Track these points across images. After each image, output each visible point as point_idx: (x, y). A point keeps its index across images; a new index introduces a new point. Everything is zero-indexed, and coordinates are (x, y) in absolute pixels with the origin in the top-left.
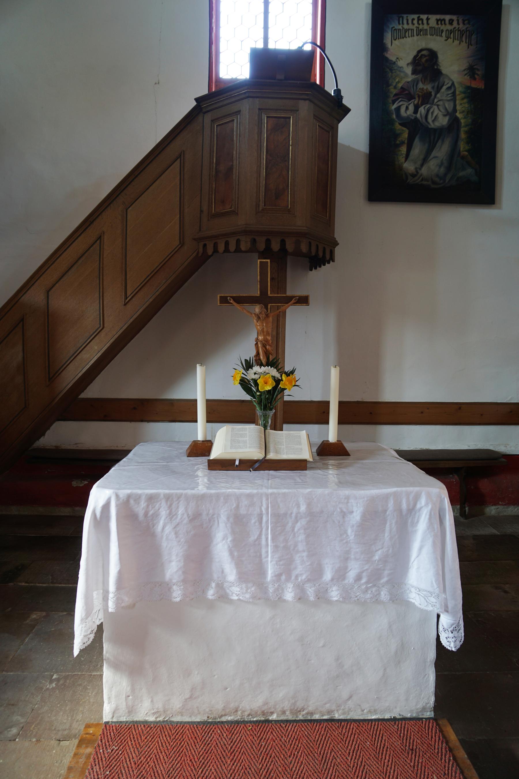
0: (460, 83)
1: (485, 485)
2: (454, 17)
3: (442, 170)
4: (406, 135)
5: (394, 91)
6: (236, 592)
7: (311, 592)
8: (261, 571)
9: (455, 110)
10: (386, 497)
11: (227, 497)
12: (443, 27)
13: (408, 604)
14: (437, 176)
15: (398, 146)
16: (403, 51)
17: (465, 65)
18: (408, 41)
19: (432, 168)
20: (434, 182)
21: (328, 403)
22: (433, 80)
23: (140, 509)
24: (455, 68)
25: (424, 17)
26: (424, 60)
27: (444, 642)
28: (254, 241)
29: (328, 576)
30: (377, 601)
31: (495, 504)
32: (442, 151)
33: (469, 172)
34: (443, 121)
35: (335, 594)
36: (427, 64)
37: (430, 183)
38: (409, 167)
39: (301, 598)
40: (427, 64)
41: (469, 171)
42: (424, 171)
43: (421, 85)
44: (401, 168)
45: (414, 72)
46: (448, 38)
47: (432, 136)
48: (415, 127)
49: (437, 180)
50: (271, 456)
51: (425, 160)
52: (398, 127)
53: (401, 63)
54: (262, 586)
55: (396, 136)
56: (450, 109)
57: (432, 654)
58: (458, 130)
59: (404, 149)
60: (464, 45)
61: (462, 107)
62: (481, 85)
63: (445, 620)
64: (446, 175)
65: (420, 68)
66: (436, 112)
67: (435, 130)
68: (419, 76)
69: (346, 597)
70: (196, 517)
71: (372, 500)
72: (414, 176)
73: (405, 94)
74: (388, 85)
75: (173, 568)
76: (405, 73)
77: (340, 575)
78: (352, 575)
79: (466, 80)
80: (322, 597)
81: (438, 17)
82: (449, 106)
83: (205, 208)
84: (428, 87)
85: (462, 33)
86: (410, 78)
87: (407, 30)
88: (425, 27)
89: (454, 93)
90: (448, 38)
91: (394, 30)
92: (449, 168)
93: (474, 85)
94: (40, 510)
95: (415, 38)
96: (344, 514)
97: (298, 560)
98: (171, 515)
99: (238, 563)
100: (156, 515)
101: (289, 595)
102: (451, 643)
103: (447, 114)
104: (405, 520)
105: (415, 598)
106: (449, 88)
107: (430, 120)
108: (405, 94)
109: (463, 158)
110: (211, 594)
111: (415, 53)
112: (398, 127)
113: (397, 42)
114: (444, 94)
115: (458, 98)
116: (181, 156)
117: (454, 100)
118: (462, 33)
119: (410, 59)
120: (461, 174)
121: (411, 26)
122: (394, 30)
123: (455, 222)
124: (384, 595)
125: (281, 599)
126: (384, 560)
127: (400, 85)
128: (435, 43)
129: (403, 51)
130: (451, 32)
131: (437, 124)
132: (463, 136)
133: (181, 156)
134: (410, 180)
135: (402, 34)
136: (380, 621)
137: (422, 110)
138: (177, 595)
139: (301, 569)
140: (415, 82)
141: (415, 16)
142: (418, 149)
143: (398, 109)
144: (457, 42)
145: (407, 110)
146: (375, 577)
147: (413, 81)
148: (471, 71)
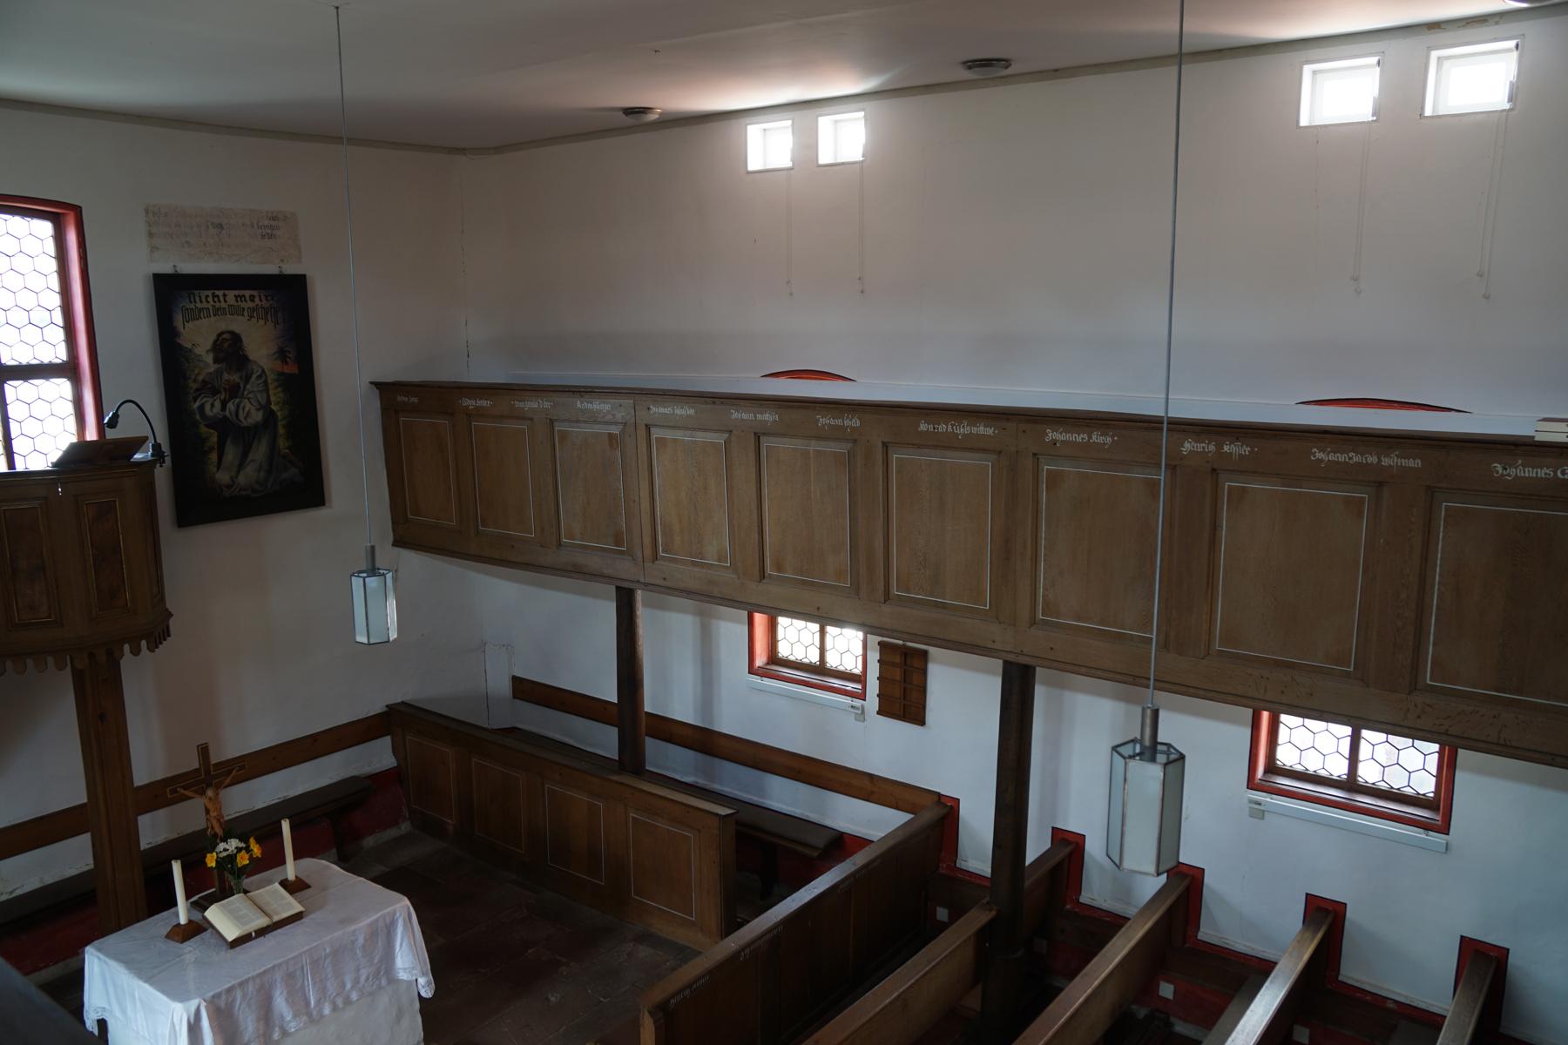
2: (255, 293)
3: (262, 474)
4: (215, 439)
5: (194, 386)
7: (340, 1002)
8: (308, 1004)
9: (269, 402)
10: (377, 921)
12: (243, 305)
13: (399, 981)
16: (199, 336)
18: (204, 321)
21: (296, 858)
23: (222, 1003)
25: (220, 293)
27: (423, 994)
29: (349, 986)
30: (380, 987)
32: (260, 452)
34: (257, 417)
35: (354, 996)
36: (230, 350)
38: (223, 477)
39: (335, 1008)
40: (230, 350)
42: (242, 479)
43: (226, 376)
45: (216, 361)
46: (251, 317)
48: (225, 427)
50: (276, 918)
51: (241, 466)
52: (203, 429)
53: (198, 351)
54: (309, 1015)
56: (263, 400)
57: (417, 1005)
59: (214, 456)
61: (276, 396)
63: (422, 981)
66: (248, 406)
67: (248, 428)
71: (370, 925)
72: (229, 487)
73: (209, 388)
77: (356, 981)
78: (363, 978)
80: (348, 1002)
81: (237, 292)
82: (262, 398)
84: (235, 378)
87: (201, 310)
88: (223, 305)
89: (266, 382)
90: (251, 317)
93: (287, 370)
95: (213, 319)
96: (353, 942)
97: (329, 984)
98: (244, 996)
100: (234, 1000)
102: (427, 993)
103: (261, 407)
104: (390, 929)
105: (403, 976)
106: (259, 377)
107: (241, 417)
108: (209, 388)
110: (276, 1036)
112: (203, 429)
113: (190, 325)
114: (254, 385)
117: (267, 390)
119: (209, 344)
121: (205, 305)
123: (284, 531)
124: (384, 982)
125: (322, 1016)
127: (201, 378)
128: (238, 324)
129: (199, 336)
130: (254, 310)
131: (250, 421)
132: (281, 431)
135: (195, 315)
136: (384, 1000)
137: (231, 406)
139: (332, 987)
140: (219, 373)
141: (209, 293)
142: (231, 453)
143: (202, 407)
145: (213, 408)
146: (377, 975)
148: (282, 354)
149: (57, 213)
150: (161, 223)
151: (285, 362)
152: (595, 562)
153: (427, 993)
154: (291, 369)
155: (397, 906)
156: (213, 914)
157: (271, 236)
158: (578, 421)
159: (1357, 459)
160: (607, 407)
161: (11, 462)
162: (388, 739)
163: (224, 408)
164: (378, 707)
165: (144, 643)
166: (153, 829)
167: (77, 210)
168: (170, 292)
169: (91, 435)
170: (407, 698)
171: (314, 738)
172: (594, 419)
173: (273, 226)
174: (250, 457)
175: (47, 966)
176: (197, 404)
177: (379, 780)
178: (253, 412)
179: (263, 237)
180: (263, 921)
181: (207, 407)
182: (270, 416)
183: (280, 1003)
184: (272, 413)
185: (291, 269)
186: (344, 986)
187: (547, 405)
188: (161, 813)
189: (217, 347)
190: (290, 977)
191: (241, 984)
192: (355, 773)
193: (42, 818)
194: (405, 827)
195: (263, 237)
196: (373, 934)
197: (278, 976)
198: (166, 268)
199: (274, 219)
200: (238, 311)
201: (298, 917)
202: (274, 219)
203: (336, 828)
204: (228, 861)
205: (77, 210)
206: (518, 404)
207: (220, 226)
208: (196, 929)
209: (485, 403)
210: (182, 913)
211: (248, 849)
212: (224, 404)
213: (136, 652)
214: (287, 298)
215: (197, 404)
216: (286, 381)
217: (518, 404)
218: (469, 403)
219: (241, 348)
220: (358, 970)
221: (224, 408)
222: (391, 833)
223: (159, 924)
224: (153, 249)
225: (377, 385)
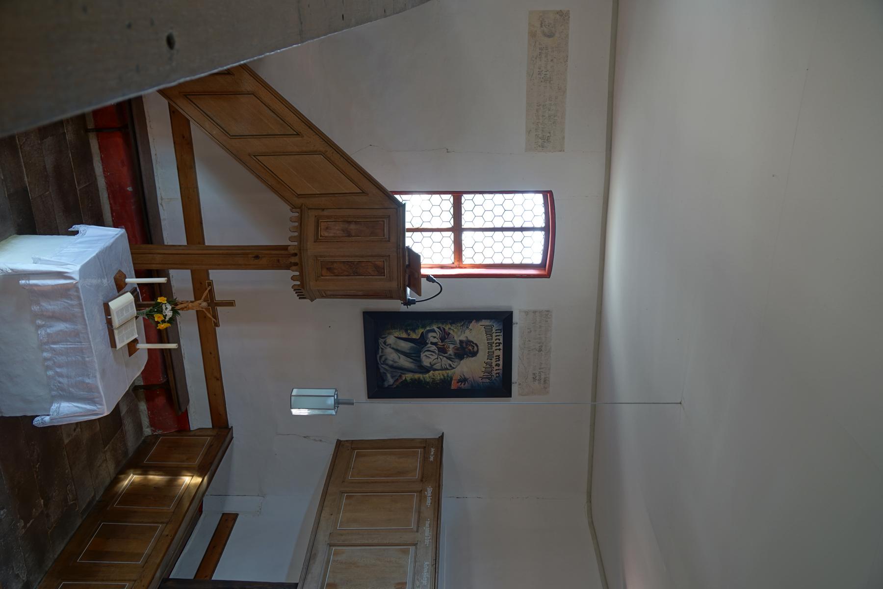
1: (161, 401)
2: (501, 367)
3: (391, 363)
4: (414, 336)
5: (447, 328)
6: (42, 332)
8: (54, 343)
9: (435, 370)
10: (99, 393)
11: (86, 329)
13: (51, 404)
14: (386, 359)
15: (406, 331)
16: (476, 333)
17: (467, 376)
19: (391, 356)
20: (381, 357)
22: (455, 354)
25: (501, 347)
26: (470, 348)
27: (37, 419)
28: (295, 255)
29: (58, 370)
31: (148, 408)
33: (391, 381)
34: (426, 362)
35: (50, 373)
36: (466, 350)
37: (380, 354)
38: (391, 339)
39: (46, 359)
42: (388, 350)
43: (452, 346)
44: (390, 334)
45: (461, 342)
47: (414, 355)
48: (422, 342)
49: (383, 359)
50: (116, 332)
51: (397, 351)
52: (421, 331)
53: (467, 332)
54: (47, 343)
55: (414, 330)
56: (437, 366)
57: (29, 414)
58: (420, 373)
59: (404, 335)
61: (438, 375)
62: (453, 387)
63: (47, 418)
64: (387, 365)
65: (464, 345)
66: (433, 358)
68: (458, 346)
69: (49, 377)
71: (97, 388)
72: (385, 343)
73: (445, 336)
74: (451, 324)
76: (459, 334)
77: (61, 375)
78: (61, 380)
79: (457, 377)
80: (48, 368)
81: (501, 357)
83: (326, 213)
84: (451, 351)
88: (494, 348)
89: (447, 369)
92: (392, 367)
96: (88, 376)
97: (64, 358)
98: (72, 306)
99: (58, 333)
100: (71, 300)
101: (45, 354)
102: (37, 422)
104: (91, 401)
105: (55, 406)
106: (450, 366)
107: (426, 353)
108: (445, 336)
109: (400, 376)
110: (39, 322)
112: (421, 331)
114: (446, 362)
115: (444, 372)
116: (363, 193)
119: (471, 338)
120: (389, 375)
121: (494, 338)
122: (492, 326)
124: (54, 393)
125: (43, 351)
127: (451, 332)
128: (482, 356)
132: (417, 376)
133: (363, 193)
134: (381, 341)
135: (489, 332)
137: (434, 348)
138: (35, 308)
140: (454, 343)
141: (501, 341)
142: (405, 346)
143: (434, 331)
144: (483, 369)
145: (433, 337)
146: (63, 390)
147: (455, 341)
148: (464, 380)
149: (546, 268)
150: (542, 317)
152: (317, 568)
153: (37, 422)
154: (454, 386)
155: (105, 407)
156: (128, 297)
157: (534, 379)
158: (415, 562)
160: (425, 582)
161: (410, 230)
162: (211, 426)
163: (432, 343)
164: (231, 422)
165: (298, 283)
166: (181, 280)
167: (548, 276)
168: (504, 319)
169: (424, 271)
170: (235, 434)
171: (220, 379)
172: (417, 573)
173: (541, 380)
174: (402, 357)
175: (112, 216)
176: (436, 329)
177: (183, 419)
178: (430, 360)
179: (534, 374)
180: (116, 322)
181: (434, 334)
182: (426, 370)
183: (61, 326)
185: (515, 389)
186: (60, 366)
187: (427, 542)
189: (469, 342)
190: (77, 334)
191: (81, 304)
192: (191, 402)
193: (201, 223)
194: (147, 431)
195: (534, 374)
196: (91, 389)
197: (79, 327)
198: (516, 319)
200: (490, 356)
201: (113, 344)
202: (545, 381)
203: (160, 384)
204: (159, 309)
205: (548, 276)
206: (427, 523)
207: (540, 350)
208: (120, 287)
209: (429, 501)
210: (132, 280)
211: (163, 321)
213: (293, 278)
214: (499, 386)
215: (436, 329)
216: (447, 382)
217: (427, 523)
218: (429, 491)
219: (468, 356)
220: (67, 377)
221: (432, 343)
222: (145, 421)
223: (128, 267)
224: (527, 313)
225: (442, 437)
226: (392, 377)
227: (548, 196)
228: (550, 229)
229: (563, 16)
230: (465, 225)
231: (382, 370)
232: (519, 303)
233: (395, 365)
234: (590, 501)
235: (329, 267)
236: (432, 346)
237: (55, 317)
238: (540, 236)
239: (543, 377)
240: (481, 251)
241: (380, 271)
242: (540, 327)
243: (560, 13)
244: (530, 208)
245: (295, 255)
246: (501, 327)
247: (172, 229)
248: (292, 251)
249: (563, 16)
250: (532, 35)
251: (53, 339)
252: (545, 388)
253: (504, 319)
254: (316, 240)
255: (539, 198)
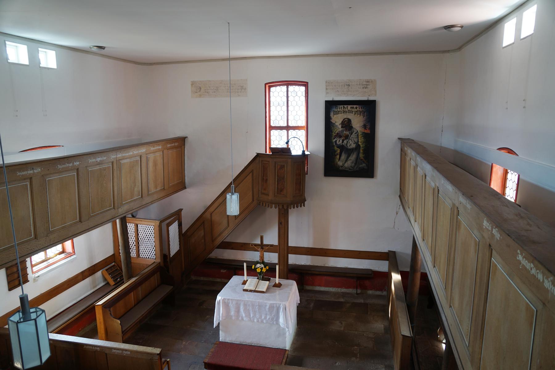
0: (360, 131)
2: (357, 106)
3: (353, 164)
5: (334, 135)
6: (245, 319)
7: (260, 320)
9: (358, 141)
12: (353, 110)
16: (337, 120)
17: (362, 124)
18: (340, 115)
20: (350, 169)
22: (349, 130)
23: (226, 301)
24: (358, 125)
25: (346, 106)
29: (263, 318)
32: (353, 157)
34: (353, 146)
35: (265, 321)
36: (347, 124)
38: (340, 163)
39: (258, 321)
40: (347, 124)
41: (364, 165)
42: (346, 165)
43: (345, 132)
44: (337, 164)
45: (342, 127)
46: (355, 114)
47: (349, 152)
48: (343, 148)
51: (346, 161)
52: (336, 148)
53: (337, 124)
54: (250, 318)
55: (335, 151)
58: (360, 149)
59: (338, 156)
60: (362, 116)
61: (361, 140)
62: (369, 132)
68: (344, 129)
70: (237, 304)
71: (271, 304)
72: (342, 167)
75: (232, 313)
77: (265, 318)
78: (268, 318)
79: (363, 130)
80: (262, 322)
82: (356, 140)
84: (348, 133)
85: (361, 112)
86: (341, 129)
89: (358, 135)
90: (355, 114)
91: (334, 111)
92: (356, 164)
93: (366, 132)
94: (211, 279)
96: (266, 306)
98: (232, 303)
99: (245, 313)
101: (255, 321)
103: (355, 143)
107: (348, 145)
108: (339, 135)
111: (342, 120)
112: (336, 148)
114: (354, 136)
117: (358, 138)
118: (361, 112)
119: (340, 122)
122: (334, 111)
125: (254, 321)
126: (274, 316)
128: (350, 116)
129: (337, 120)
131: (351, 147)
132: (361, 151)
134: (341, 168)
135: (337, 113)
137: (345, 142)
138: (233, 318)
139: (258, 316)
140: (342, 131)
142: (343, 157)
145: (339, 141)
146: (272, 319)
148: (365, 126)
150: (330, 85)
151: (365, 128)
154: (368, 131)
157: (366, 88)
159: (540, 277)
162: (387, 262)
163: (343, 142)
164: (385, 250)
167: (307, 83)
168: (330, 105)
173: (367, 84)
174: (350, 158)
179: (363, 88)
181: (338, 141)
184: (359, 145)
185: (371, 98)
186: (261, 317)
188: (309, 257)
189: (343, 123)
190: (245, 305)
196: (272, 307)
198: (330, 99)
199: (368, 82)
202: (368, 82)
207: (349, 85)
212: (343, 141)
214: (369, 108)
216: (365, 135)
219: (351, 124)
220: (266, 315)
221: (343, 142)
222: (378, 293)
224: (327, 93)
226: (362, 164)
227: (270, 85)
228: (288, 83)
229: (193, 83)
230: (285, 125)
231: (358, 169)
232: (321, 98)
233: (354, 162)
234: (448, 51)
235: (280, 190)
236: (350, 143)
237: (238, 311)
238: (291, 88)
239: (365, 83)
240: (298, 117)
241: (282, 167)
242: (335, 86)
243: (192, 85)
244: (277, 94)
245: (283, 206)
246: (334, 106)
247: (272, 258)
248: (281, 207)
249: (193, 83)
250: (200, 96)
251: (248, 315)
252: (372, 81)
253: (330, 105)
254: (268, 195)
255: (272, 89)
